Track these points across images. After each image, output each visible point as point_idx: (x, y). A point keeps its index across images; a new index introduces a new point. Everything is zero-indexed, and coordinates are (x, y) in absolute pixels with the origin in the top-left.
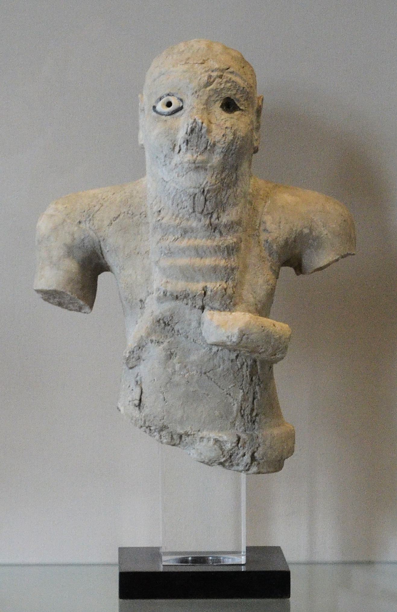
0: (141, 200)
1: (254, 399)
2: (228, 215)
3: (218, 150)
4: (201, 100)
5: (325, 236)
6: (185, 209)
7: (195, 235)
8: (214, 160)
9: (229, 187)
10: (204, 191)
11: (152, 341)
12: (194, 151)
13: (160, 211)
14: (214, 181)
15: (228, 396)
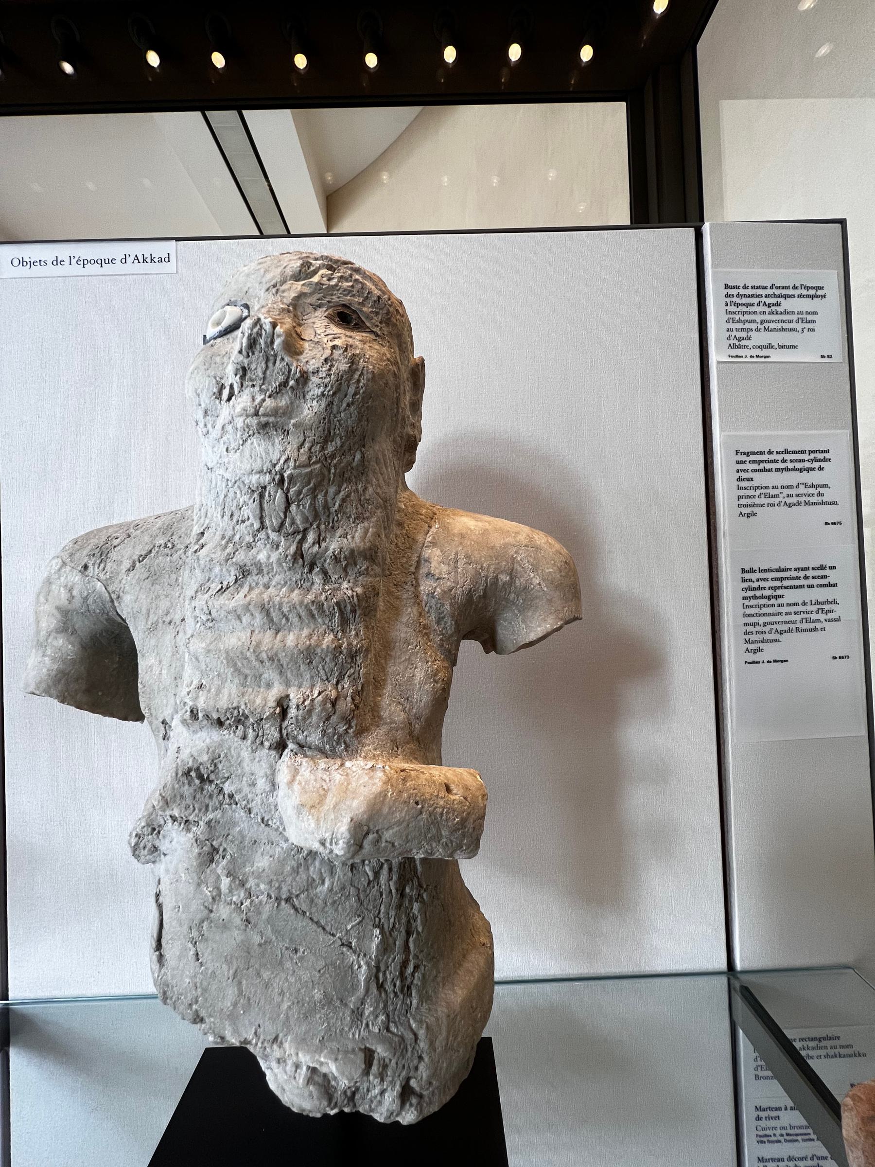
1: (409, 934)
2: (345, 536)
3: (314, 389)
5: (537, 587)
6: (247, 523)
7: (266, 579)
8: (306, 412)
10: (282, 480)
11: (174, 819)
12: (257, 389)
14: (303, 458)
15: (345, 949)
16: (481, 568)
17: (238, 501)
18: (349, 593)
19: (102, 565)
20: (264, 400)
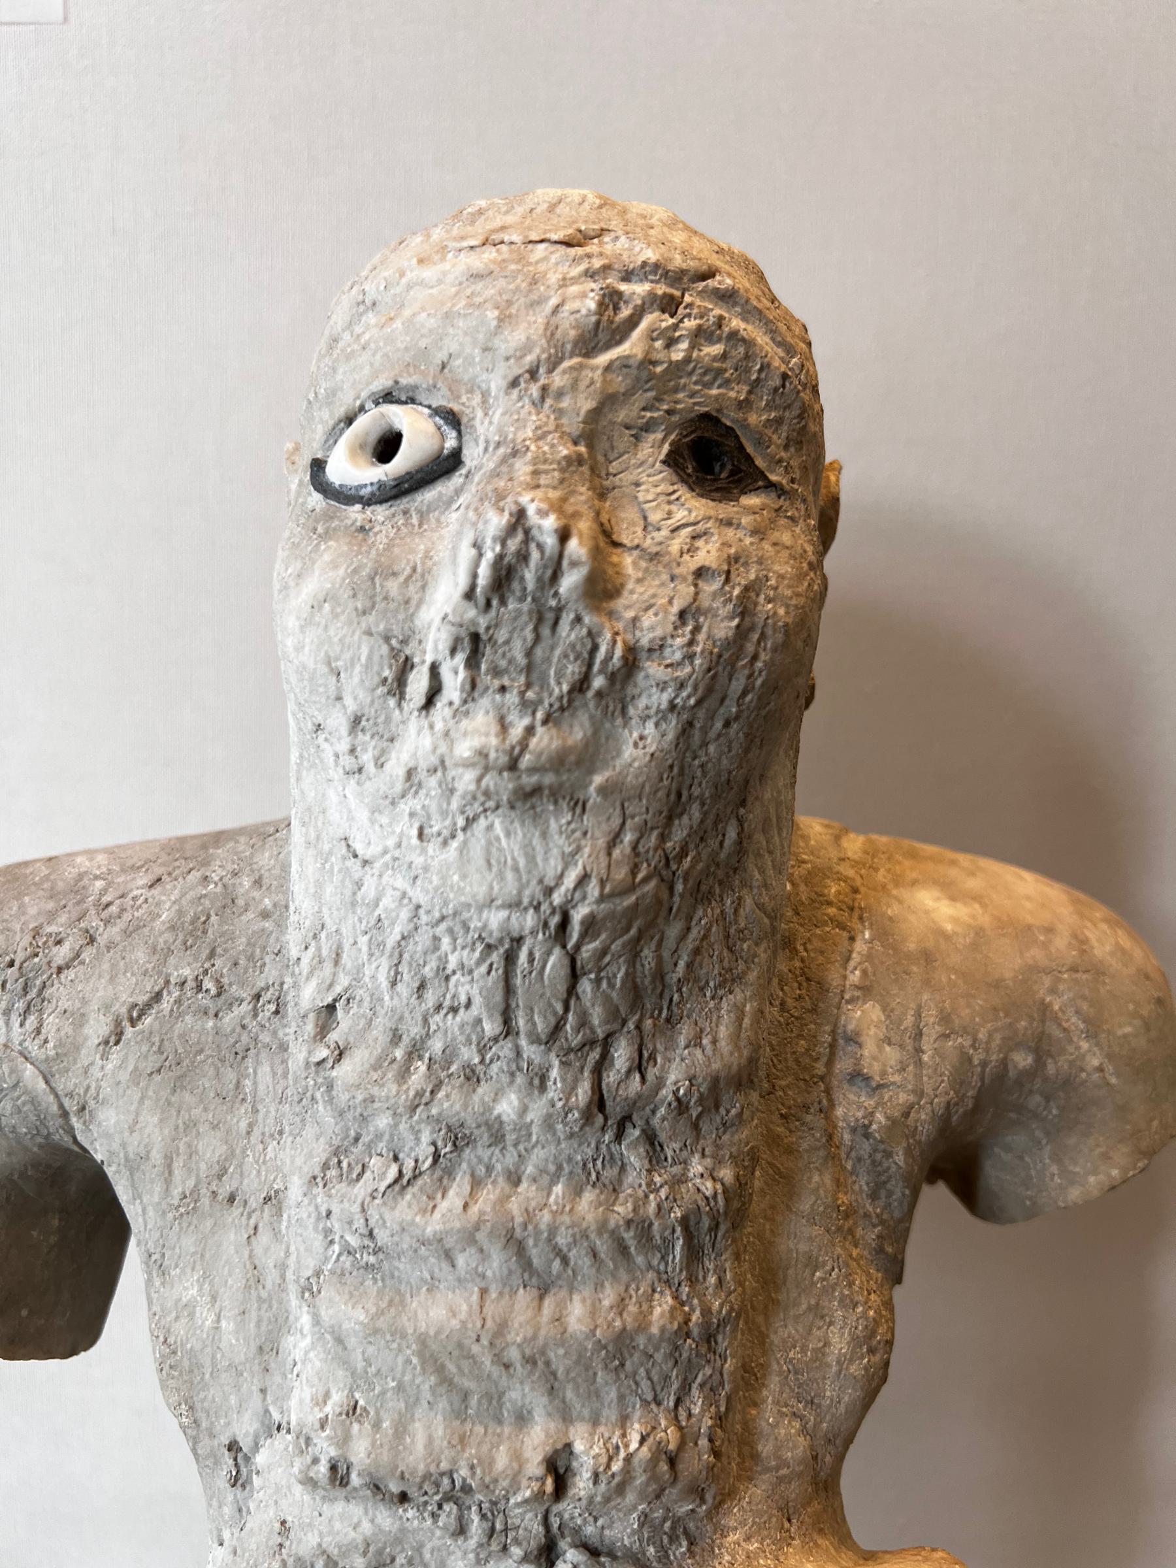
0: (267, 924)
4: (559, 413)
5: (1096, 1076)
7: (511, 1158)
8: (628, 752)
9: (700, 895)
12: (512, 698)
13: (331, 1008)
14: (621, 874)
16: (973, 1046)
17: (444, 960)
18: (708, 1187)
19: (32, 1020)
20: (530, 731)
